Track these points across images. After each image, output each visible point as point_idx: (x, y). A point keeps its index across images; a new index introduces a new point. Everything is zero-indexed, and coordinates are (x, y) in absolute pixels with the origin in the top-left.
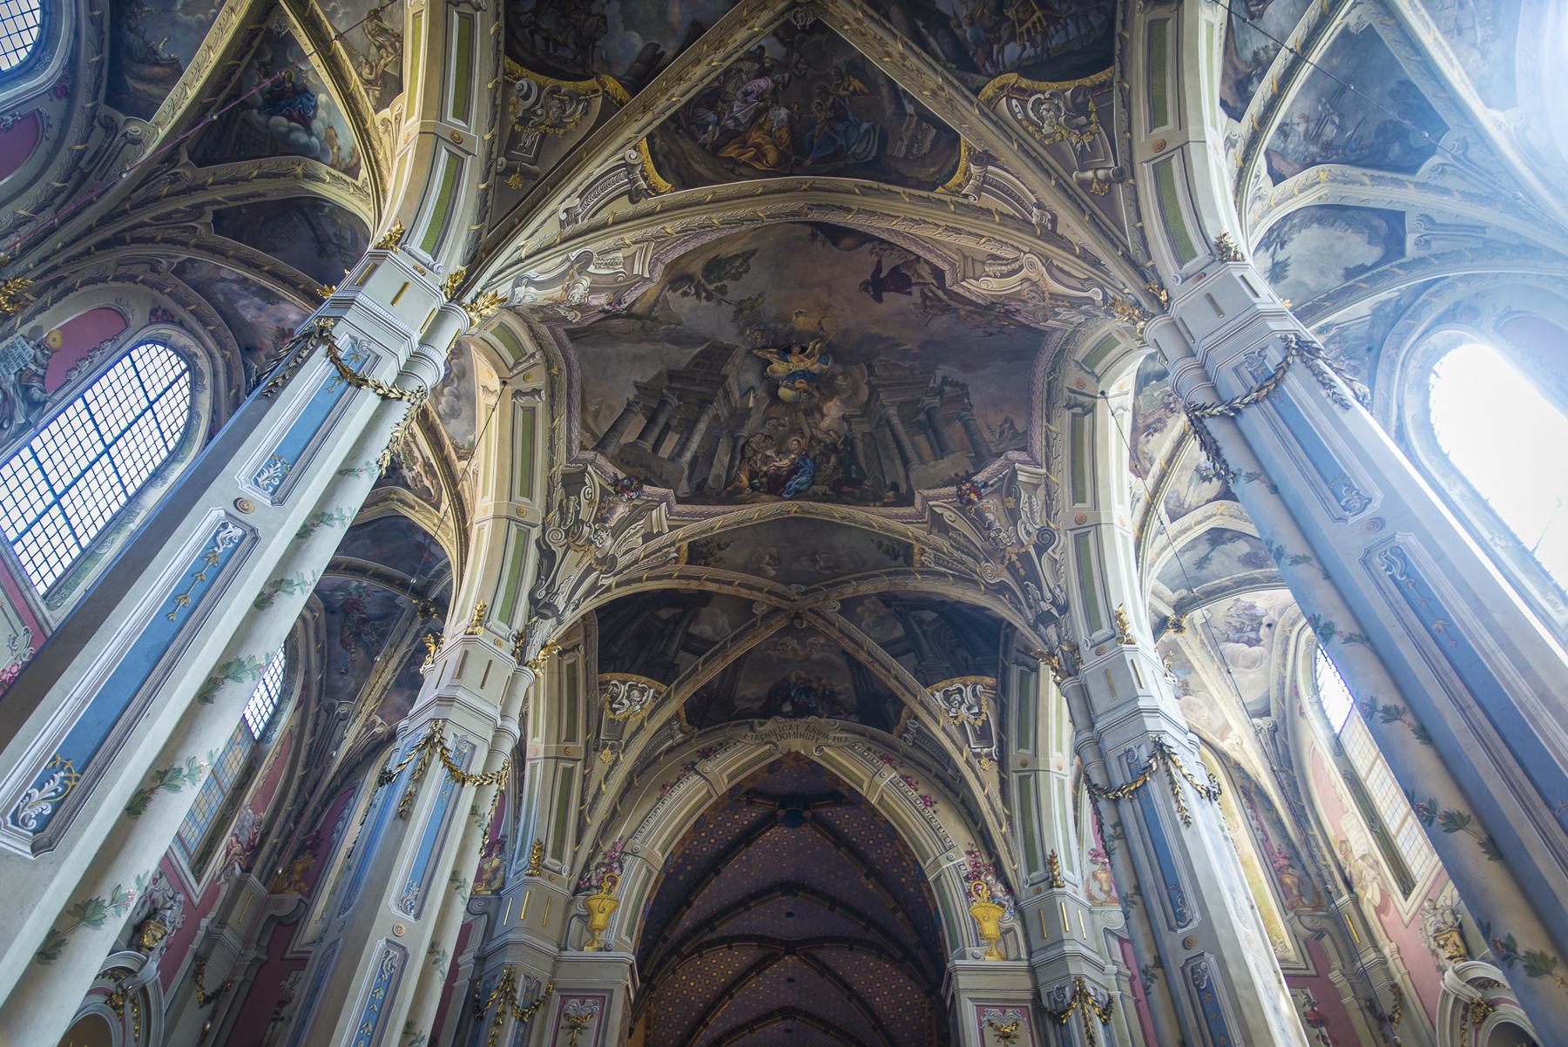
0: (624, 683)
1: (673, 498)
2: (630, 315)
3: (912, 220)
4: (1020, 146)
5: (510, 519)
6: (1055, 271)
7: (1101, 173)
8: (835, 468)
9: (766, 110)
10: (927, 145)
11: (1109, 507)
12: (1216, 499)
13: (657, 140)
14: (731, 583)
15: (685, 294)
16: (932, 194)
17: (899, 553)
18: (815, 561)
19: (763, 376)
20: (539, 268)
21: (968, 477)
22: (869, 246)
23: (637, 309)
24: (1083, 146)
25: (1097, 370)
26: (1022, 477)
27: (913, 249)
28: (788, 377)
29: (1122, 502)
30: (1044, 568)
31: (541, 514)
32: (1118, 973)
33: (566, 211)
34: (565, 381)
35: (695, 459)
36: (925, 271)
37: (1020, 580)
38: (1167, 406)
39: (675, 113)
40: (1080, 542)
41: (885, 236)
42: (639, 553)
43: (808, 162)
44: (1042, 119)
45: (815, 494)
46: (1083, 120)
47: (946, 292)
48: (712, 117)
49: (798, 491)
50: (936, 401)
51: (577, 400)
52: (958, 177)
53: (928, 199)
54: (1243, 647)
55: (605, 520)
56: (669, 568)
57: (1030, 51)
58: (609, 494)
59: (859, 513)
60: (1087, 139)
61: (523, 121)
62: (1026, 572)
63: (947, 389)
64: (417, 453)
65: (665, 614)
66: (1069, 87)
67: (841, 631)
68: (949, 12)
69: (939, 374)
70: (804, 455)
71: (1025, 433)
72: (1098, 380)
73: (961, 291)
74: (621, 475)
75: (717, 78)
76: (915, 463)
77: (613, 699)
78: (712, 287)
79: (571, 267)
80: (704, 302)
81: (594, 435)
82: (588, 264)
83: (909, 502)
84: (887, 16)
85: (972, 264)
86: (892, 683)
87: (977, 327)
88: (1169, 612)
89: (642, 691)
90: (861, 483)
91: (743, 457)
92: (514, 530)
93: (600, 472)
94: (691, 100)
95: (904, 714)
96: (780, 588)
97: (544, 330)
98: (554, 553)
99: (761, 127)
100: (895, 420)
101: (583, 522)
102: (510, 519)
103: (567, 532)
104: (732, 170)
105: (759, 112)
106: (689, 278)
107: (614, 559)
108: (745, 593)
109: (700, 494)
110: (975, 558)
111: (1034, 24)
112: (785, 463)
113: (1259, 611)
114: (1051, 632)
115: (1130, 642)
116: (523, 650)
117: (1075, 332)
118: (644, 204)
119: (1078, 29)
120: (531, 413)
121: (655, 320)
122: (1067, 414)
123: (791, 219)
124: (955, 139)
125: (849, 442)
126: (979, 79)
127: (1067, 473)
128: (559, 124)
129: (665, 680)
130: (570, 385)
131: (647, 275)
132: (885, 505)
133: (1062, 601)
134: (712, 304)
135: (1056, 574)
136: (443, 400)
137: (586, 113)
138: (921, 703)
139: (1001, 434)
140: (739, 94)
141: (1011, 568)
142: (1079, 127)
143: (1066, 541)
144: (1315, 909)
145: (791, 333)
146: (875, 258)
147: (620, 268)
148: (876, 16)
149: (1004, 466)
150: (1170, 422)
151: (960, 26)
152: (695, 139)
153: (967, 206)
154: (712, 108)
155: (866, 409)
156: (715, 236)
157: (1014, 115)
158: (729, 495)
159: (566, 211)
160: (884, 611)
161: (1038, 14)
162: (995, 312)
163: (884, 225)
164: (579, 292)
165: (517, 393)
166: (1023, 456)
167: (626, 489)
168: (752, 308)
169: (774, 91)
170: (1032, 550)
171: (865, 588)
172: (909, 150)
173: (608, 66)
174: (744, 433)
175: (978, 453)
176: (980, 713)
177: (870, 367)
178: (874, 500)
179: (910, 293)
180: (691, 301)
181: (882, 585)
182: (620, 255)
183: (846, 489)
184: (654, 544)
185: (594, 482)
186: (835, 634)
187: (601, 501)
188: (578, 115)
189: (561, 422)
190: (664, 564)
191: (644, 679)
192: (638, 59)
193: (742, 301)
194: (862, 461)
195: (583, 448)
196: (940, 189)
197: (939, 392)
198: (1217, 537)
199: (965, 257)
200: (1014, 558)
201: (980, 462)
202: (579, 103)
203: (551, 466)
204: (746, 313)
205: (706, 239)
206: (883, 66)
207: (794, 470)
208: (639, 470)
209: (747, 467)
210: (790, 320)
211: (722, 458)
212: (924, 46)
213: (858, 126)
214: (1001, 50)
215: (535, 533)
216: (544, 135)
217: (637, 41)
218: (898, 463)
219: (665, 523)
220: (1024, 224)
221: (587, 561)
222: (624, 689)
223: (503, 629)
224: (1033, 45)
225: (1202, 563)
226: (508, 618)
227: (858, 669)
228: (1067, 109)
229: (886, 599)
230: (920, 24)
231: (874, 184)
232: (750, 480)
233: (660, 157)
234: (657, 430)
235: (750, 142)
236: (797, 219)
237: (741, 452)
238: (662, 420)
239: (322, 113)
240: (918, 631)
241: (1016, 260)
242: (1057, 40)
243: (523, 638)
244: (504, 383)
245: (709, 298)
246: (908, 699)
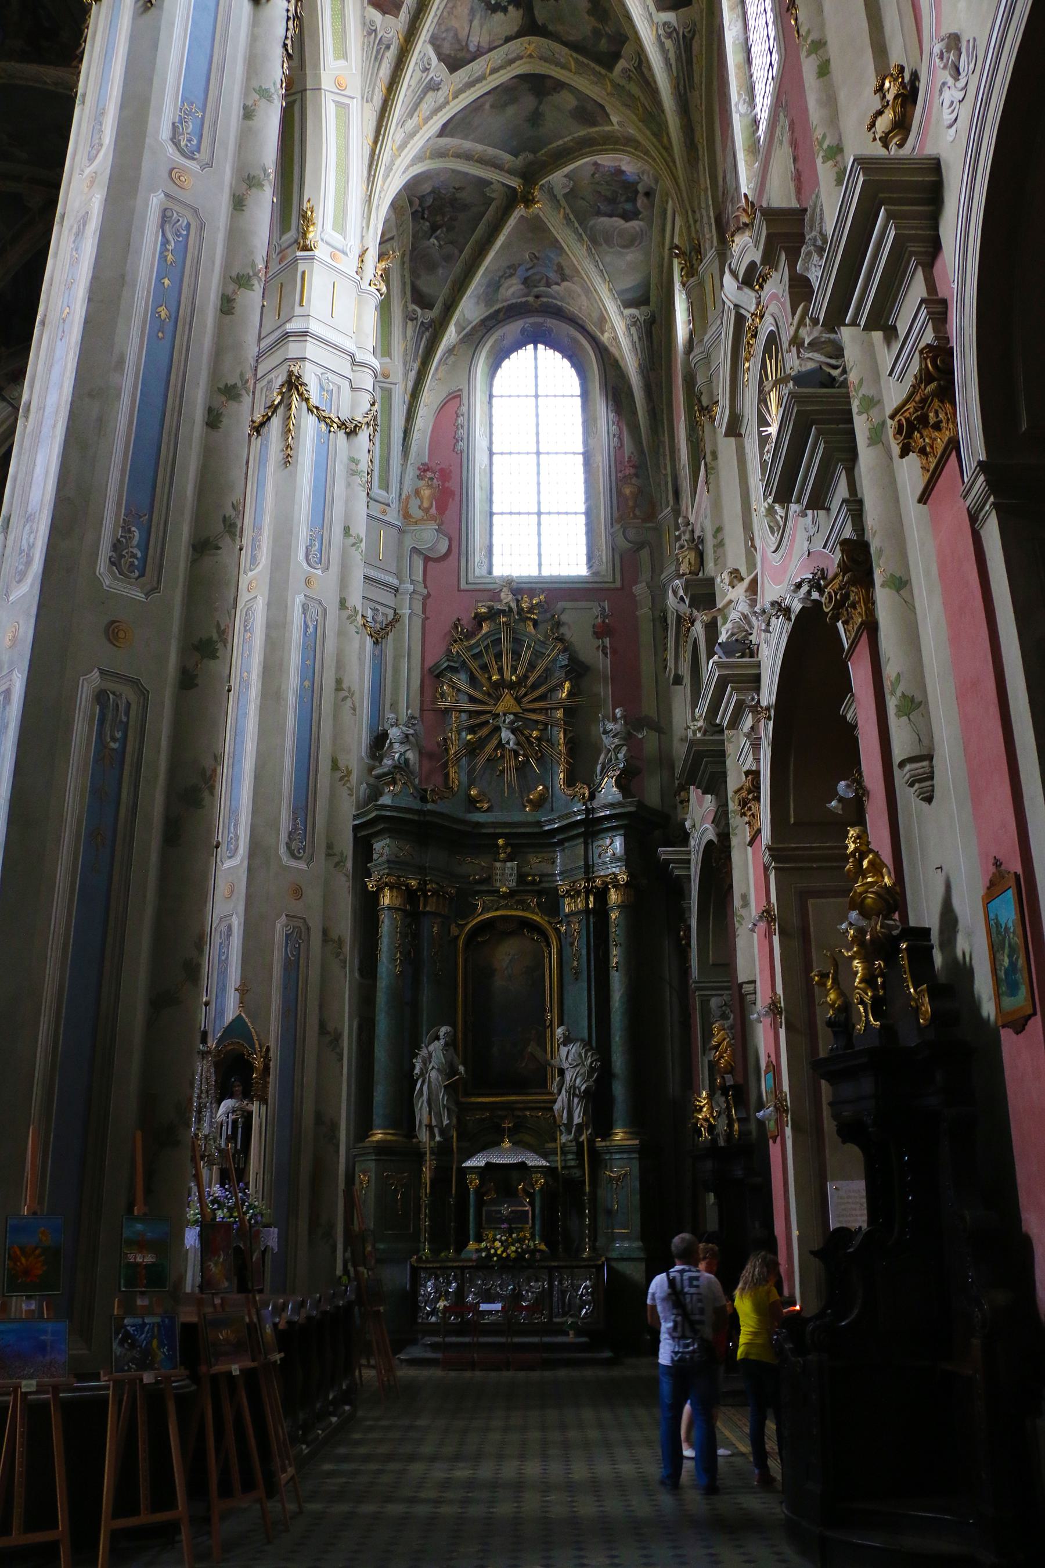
11: (317, 66)
12: (519, 35)
29: (342, 53)
32: (414, 592)
88: (515, 183)
113: (633, 178)
115: (306, 248)
144: (644, 520)
198: (537, 85)
225: (535, 118)
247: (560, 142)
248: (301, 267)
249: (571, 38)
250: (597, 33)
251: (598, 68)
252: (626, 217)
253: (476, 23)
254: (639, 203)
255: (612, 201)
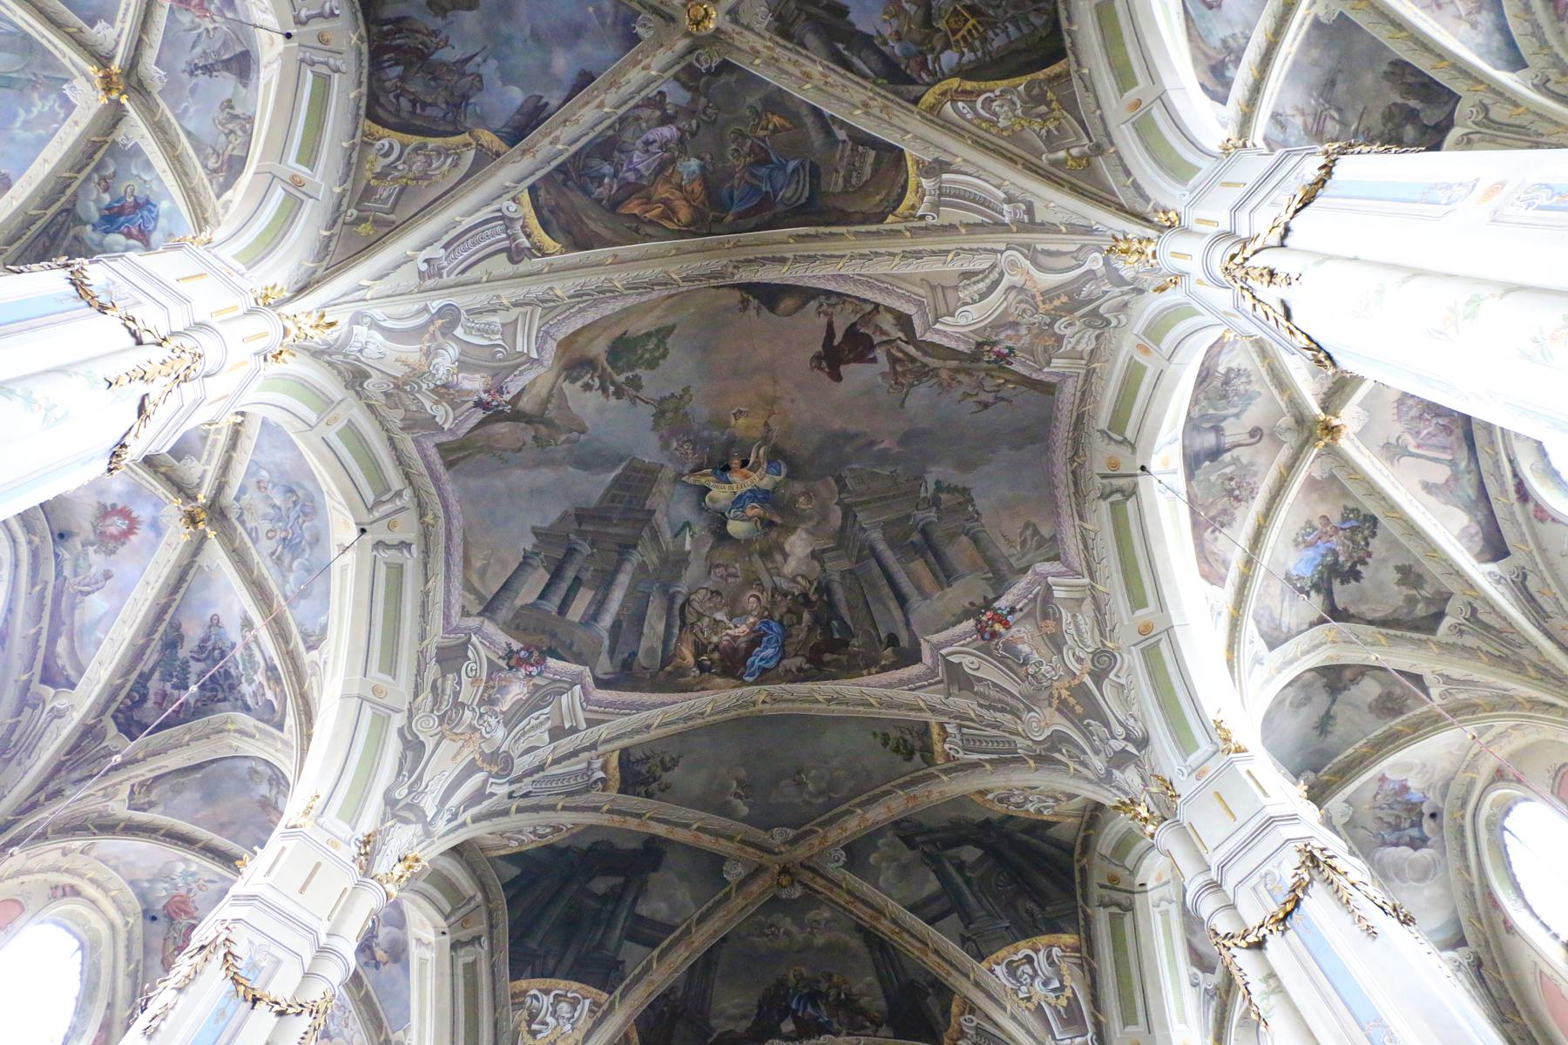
0: (547, 992)
1: (589, 680)
2: (517, 416)
3: (862, 256)
4: (975, 142)
5: (363, 699)
6: (1043, 259)
7: (1074, 151)
8: (810, 629)
9: (673, 161)
10: (868, 170)
12: (1322, 621)
13: (542, 193)
14: (687, 826)
15: (587, 387)
16: (881, 227)
17: (911, 745)
18: (800, 785)
19: (701, 508)
20: (391, 310)
21: (988, 604)
22: (813, 304)
23: (526, 404)
24: (1049, 131)
25: (1130, 433)
26: (1059, 593)
27: (869, 295)
28: (734, 503)
30: (1108, 699)
31: (409, 697)
33: (427, 261)
34: (442, 532)
35: (616, 626)
36: (887, 321)
37: (1077, 720)
38: (1230, 493)
39: (563, 164)
40: (1151, 657)
41: (831, 286)
42: (545, 753)
43: (729, 218)
44: (995, 114)
45: (787, 671)
46: (1043, 109)
47: (919, 345)
48: (607, 169)
49: (764, 671)
50: (932, 515)
51: (457, 555)
52: (910, 199)
53: (878, 233)
54: (1405, 851)
55: (492, 702)
56: (595, 797)
57: (969, 56)
58: (501, 669)
59: (847, 688)
60: (1051, 125)
61: (380, 176)
62: (1082, 707)
63: (943, 496)
64: (258, 658)
65: (600, 885)
66: (1021, 83)
67: (850, 892)
68: (871, 31)
69: (931, 480)
70: (767, 617)
71: (1054, 538)
72: (1133, 446)
73: (936, 339)
74: (516, 646)
75: (611, 127)
76: (915, 601)
77: (532, 1017)
78: (621, 378)
79: (431, 321)
80: (613, 400)
81: (480, 597)
82: (455, 322)
83: (913, 657)
84: (802, 44)
85: (941, 294)
86: (932, 961)
87: (966, 395)
89: (574, 1004)
90: (847, 644)
91: (683, 624)
92: (367, 712)
93: (490, 640)
94: (582, 149)
95: (955, 1010)
96: (759, 835)
97: (407, 442)
98: (422, 744)
99: (668, 180)
100: (881, 546)
101: (463, 705)
102: (363, 699)
103: (442, 719)
104: (636, 230)
105: (662, 166)
106: (588, 364)
107: (508, 762)
108: (707, 841)
109: (626, 675)
110: (1015, 712)
111: (969, 31)
112: (742, 630)
113: (1415, 796)
114: (1130, 777)
115: (1238, 750)
116: (370, 863)
117: (1090, 373)
118: (526, 265)
119: (1020, 29)
120: (397, 572)
121: (549, 424)
122: (1104, 506)
123: (713, 282)
124: (899, 154)
125: (824, 588)
126: (915, 90)
127: (1117, 578)
128: (424, 176)
129: (606, 985)
130: (449, 537)
131: (534, 355)
132: (884, 669)
133: (1139, 734)
134: (625, 402)
135: (1126, 702)
136: (292, 577)
137: (455, 165)
138: (977, 984)
139: (1024, 543)
140: (639, 143)
141: (1064, 708)
142: (1039, 116)
143: (1132, 661)
145: (732, 442)
146: (824, 320)
147: (497, 339)
148: (790, 46)
149: (1032, 583)
150: (1238, 513)
151: (886, 44)
152: (588, 193)
153: (926, 228)
154: (607, 158)
155: (842, 537)
156: (617, 306)
157: (963, 116)
158: (667, 678)
159: (427, 261)
160: (907, 855)
161: (972, 21)
162: (984, 357)
163: (830, 270)
164: (446, 361)
165: (379, 545)
166: (1056, 567)
167: (522, 662)
168: (677, 410)
169: (681, 140)
170: (1087, 680)
171: (878, 814)
172: (847, 180)
173: (482, 121)
174: (682, 588)
175: (996, 571)
176: (1062, 988)
177: (839, 480)
178: (868, 666)
179: (874, 360)
180: (594, 399)
181: (895, 806)
182: (496, 319)
183: (827, 657)
184: (567, 744)
185: (480, 654)
186: (843, 899)
187: (490, 677)
188: (446, 167)
189: (437, 585)
190: (588, 789)
191: (575, 985)
192: (519, 111)
193: (663, 400)
194: (844, 610)
195: (465, 613)
196: (890, 218)
197: (935, 502)
198: (1334, 678)
199: (933, 288)
200: (1065, 693)
201: (1000, 583)
202: (448, 156)
203: (423, 637)
204: (669, 414)
205: (610, 308)
206: (806, 94)
207: (755, 641)
208: (540, 640)
209: (689, 638)
210: (727, 425)
211: (655, 625)
212: (848, 66)
213: (783, 168)
214: (937, 59)
215: (398, 720)
216: (403, 190)
217: (516, 95)
218: (893, 605)
219: (581, 715)
220: (999, 226)
221: (468, 755)
222: (547, 1001)
223: (343, 830)
224: (972, 49)
225: (1324, 724)
226: (352, 814)
227: (879, 946)
228: (1024, 102)
229: (908, 831)
230: (840, 46)
231: (811, 230)
232: (697, 655)
233: (545, 212)
234: (564, 587)
235: (656, 197)
236: (721, 282)
237: (681, 615)
238: (570, 573)
239: (162, 222)
240: (959, 880)
241: (993, 266)
242: (998, 42)
243: (369, 847)
244: (363, 531)
245: (619, 394)
246: (956, 981)
247: (1350, 751)
248: (1241, 768)
249: (1378, 615)
250: (1411, 601)
251: (1416, 635)
252: (1417, 843)
253: (1286, 604)
254: (1425, 827)
255: (1396, 828)
